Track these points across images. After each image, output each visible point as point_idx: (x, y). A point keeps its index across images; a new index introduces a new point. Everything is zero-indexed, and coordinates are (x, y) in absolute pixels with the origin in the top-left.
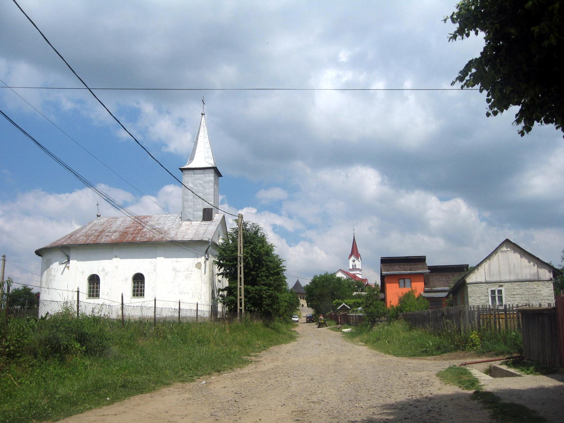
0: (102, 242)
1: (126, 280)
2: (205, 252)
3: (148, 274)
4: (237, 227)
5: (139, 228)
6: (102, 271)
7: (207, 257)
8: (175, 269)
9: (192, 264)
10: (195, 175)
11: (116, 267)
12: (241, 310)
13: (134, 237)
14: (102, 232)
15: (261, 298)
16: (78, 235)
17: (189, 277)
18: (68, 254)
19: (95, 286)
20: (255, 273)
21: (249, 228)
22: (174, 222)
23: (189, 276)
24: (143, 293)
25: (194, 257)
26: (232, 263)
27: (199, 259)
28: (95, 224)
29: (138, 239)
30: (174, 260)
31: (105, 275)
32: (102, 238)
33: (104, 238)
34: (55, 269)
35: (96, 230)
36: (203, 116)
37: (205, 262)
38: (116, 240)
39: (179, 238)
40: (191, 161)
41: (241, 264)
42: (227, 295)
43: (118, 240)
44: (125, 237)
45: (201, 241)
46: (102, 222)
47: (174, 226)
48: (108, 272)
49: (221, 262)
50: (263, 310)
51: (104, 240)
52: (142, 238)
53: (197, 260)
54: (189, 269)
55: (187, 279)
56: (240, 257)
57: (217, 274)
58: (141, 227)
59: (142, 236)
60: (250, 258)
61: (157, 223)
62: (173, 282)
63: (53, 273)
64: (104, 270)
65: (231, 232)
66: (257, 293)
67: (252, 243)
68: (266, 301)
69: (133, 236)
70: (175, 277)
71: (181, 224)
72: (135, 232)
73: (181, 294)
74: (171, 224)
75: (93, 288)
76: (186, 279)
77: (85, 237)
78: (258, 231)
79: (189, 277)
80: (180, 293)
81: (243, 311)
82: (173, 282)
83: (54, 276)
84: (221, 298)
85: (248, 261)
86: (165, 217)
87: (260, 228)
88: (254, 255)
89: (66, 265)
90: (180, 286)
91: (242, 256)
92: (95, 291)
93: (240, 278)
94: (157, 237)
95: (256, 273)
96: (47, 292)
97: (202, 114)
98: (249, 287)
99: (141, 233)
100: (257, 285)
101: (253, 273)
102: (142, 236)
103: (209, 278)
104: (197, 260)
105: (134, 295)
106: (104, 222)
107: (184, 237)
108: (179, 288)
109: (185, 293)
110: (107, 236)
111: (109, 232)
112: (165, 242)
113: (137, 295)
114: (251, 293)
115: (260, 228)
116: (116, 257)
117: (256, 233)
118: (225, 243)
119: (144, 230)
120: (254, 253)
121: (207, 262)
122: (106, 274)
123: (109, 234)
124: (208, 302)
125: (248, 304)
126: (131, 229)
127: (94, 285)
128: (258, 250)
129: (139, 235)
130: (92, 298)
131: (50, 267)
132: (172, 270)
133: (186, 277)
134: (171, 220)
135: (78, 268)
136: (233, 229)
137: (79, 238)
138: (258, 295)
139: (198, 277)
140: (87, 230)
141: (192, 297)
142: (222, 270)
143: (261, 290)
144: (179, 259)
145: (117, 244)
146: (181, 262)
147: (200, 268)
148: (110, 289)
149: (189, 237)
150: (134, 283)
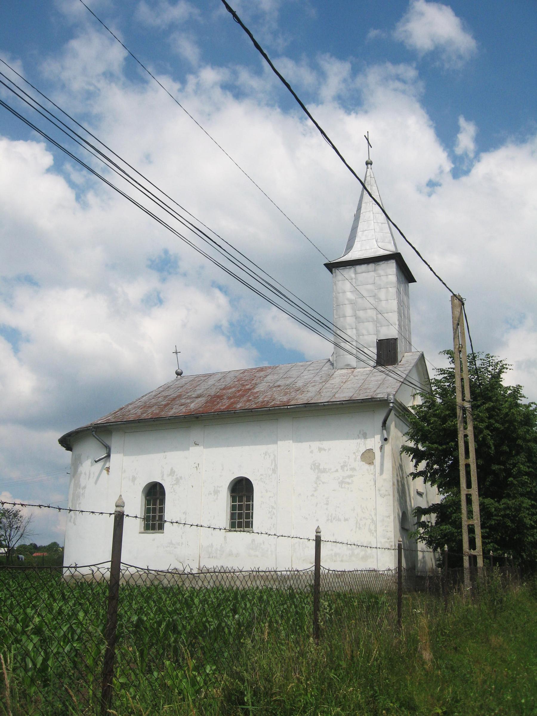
0: (168, 415)
1: (216, 492)
2: (381, 424)
3: (261, 479)
4: (453, 366)
5: (247, 387)
6: (170, 475)
7: (386, 436)
8: (316, 467)
9: (354, 453)
10: (357, 275)
11: (196, 465)
12: (473, 559)
13: (233, 403)
14: (176, 398)
15: (521, 526)
16: (130, 407)
17: (349, 483)
18: (108, 443)
19: (158, 506)
20: (500, 469)
21: (480, 366)
22: (318, 373)
23: (347, 480)
24: (251, 520)
25: (359, 438)
26: (444, 447)
27: (368, 440)
28: (168, 387)
29: (239, 406)
30: (315, 445)
31: (175, 482)
32: (173, 408)
33: (176, 409)
34: (85, 474)
35: (166, 397)
36: (369, 166)
37: (381, 448)
38: (196, 409)
39: (324, 398)
40: (348, 251)
41: (465, 428)
42: (437, 523)
43: (201, 409)
44: (216, 403)
45: (372, 401)
46: (183, 382)
47: (317, 378)
48: (181, 478)
49: (420, 447)
50: (525, 557)
51: (175, 410)
52: (248, 403)
53: (365, 444)
54: (346, 466)
55: (345, 488)
56: (464, 410)
57: (411, 474)
58: (251, 386)
59: (249, 401)
60: (486, 432)
61: (285, 376)
62: (313, 495)
63: (83, 481)
64: (174, 472)
65: (440, 377)
66: (508, 514)
67: (490, 399)
68: (532, 535)
69: (232, 400)
70: (316, 483)
71: (333, 375)
72: (238, 394)
73: (332, 522)
74: (312, 376)
75: (154, 510)
76: (342, 488)
77: (141, 409)
78: (500, 372)
79: (349, 483)
80: (328, 520)
81: (480, 562)
82: (313, 495)
83: (85, 488)
84: (421, 530)
85: (484, 439)
86: (302, 366)
87: (504, 366)
88: (497, 425)
89: (105, 464)
90: (327, 504)
91: (467, 405)
92: (157, 518)
93: (467, 466)
94: (280, 398)
95: (503, 467)
96: (72, 520)
97: (367, 163)
98: (488, 501)
99: (249, 394)
100: (508, 496)
101: (495, 467)
102: (249, 401)
103: (394, 484)
104: (365, 444)
105: (233, 525)
106: (186, 384)
107: (334, 395)
108: (327, 509)
109: (339, 520)
110: (182, 405)
111: (189, 397)
112: (292, 407)
113: (240, 526)
114: (496, 515)
115: (506, 365)
116: (196, 444)
117: (497, 377)
118: (427, 404)
119: (255, 391)
120: (497, 421)
121: (388, 448)
122: (178, 481)
123: (188, 401)
124: (393, 540)
125: (489, 543)
126: (230, 390)
127: (155, 504)
128: (505, 411)
129: (245, 398)
130: (152, 531)
131: (79, 470)
132: (311, 469)
133: (342, 483)
134: (313, 370)
135: (125, 471)
136: (442, 371)
137: (130, 411)
138: (511, 520)
139: (367, 483)
140: (151, 398)
141: (356, 527)
142: (422, 465)
143: (518, 509)
144: (326, 444)
145: (197, 417)
146: (329, 449)
147: (371, 463)
148: (185, 513)
149: (344, 395)
150: (234, 499)
